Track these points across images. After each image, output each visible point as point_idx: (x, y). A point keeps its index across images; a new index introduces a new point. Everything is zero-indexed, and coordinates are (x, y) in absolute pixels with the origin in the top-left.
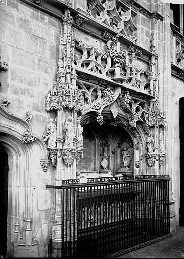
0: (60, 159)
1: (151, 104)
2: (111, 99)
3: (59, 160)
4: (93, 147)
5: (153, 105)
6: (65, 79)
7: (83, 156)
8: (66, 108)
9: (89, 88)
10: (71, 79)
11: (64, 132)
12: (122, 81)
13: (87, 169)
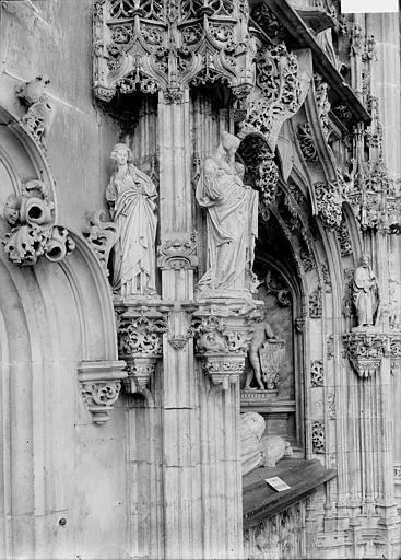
0: (186, 354)
3: (177, 362)
5: (367, 150)
11: (201, 214)
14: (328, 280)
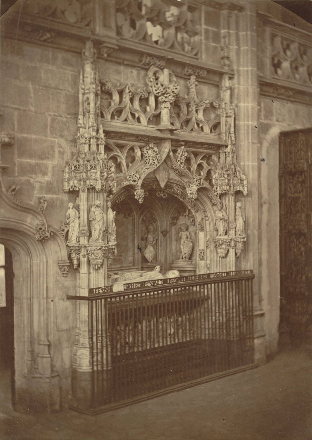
0: (86, 259)
1: (222, 156)
2: (156, 161)
4: (130, 227)
6: (90, 145)
7: (116, 251)
8: (91, 189)
9: (121, 147)
10: (98, 145)
11: (89, 222)
12: (171, 131)
13: (122, 263)
14: (206, 215)
